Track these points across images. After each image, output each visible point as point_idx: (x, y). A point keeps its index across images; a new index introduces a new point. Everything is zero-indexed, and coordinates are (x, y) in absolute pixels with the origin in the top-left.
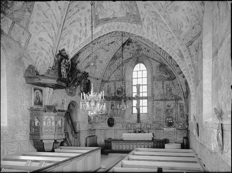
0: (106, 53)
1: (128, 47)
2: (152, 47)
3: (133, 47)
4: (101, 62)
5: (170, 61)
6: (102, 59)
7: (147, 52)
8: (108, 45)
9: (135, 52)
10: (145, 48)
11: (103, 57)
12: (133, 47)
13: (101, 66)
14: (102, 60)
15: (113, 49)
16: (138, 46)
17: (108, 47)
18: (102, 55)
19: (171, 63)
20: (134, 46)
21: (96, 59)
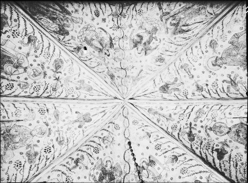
0: (188, 63)
1: (141, 32)
2: (81, 68)
3: (131, 26)
4: (213, 44)
5: (30, 30)
6: (207, 52)
7: (99, 9)
8: (176, 80)
9: (129, 12)
10: (104, 20)
11: (201, 55)
12: (131, 26)
13: (220, 33)
14: (209, 49)
15: (169, 69)
16: (119, 27)
17: (178, 76)
18: (200, 61)
19: (25, 25)
20: (128, 28)
21: (221, 58)
